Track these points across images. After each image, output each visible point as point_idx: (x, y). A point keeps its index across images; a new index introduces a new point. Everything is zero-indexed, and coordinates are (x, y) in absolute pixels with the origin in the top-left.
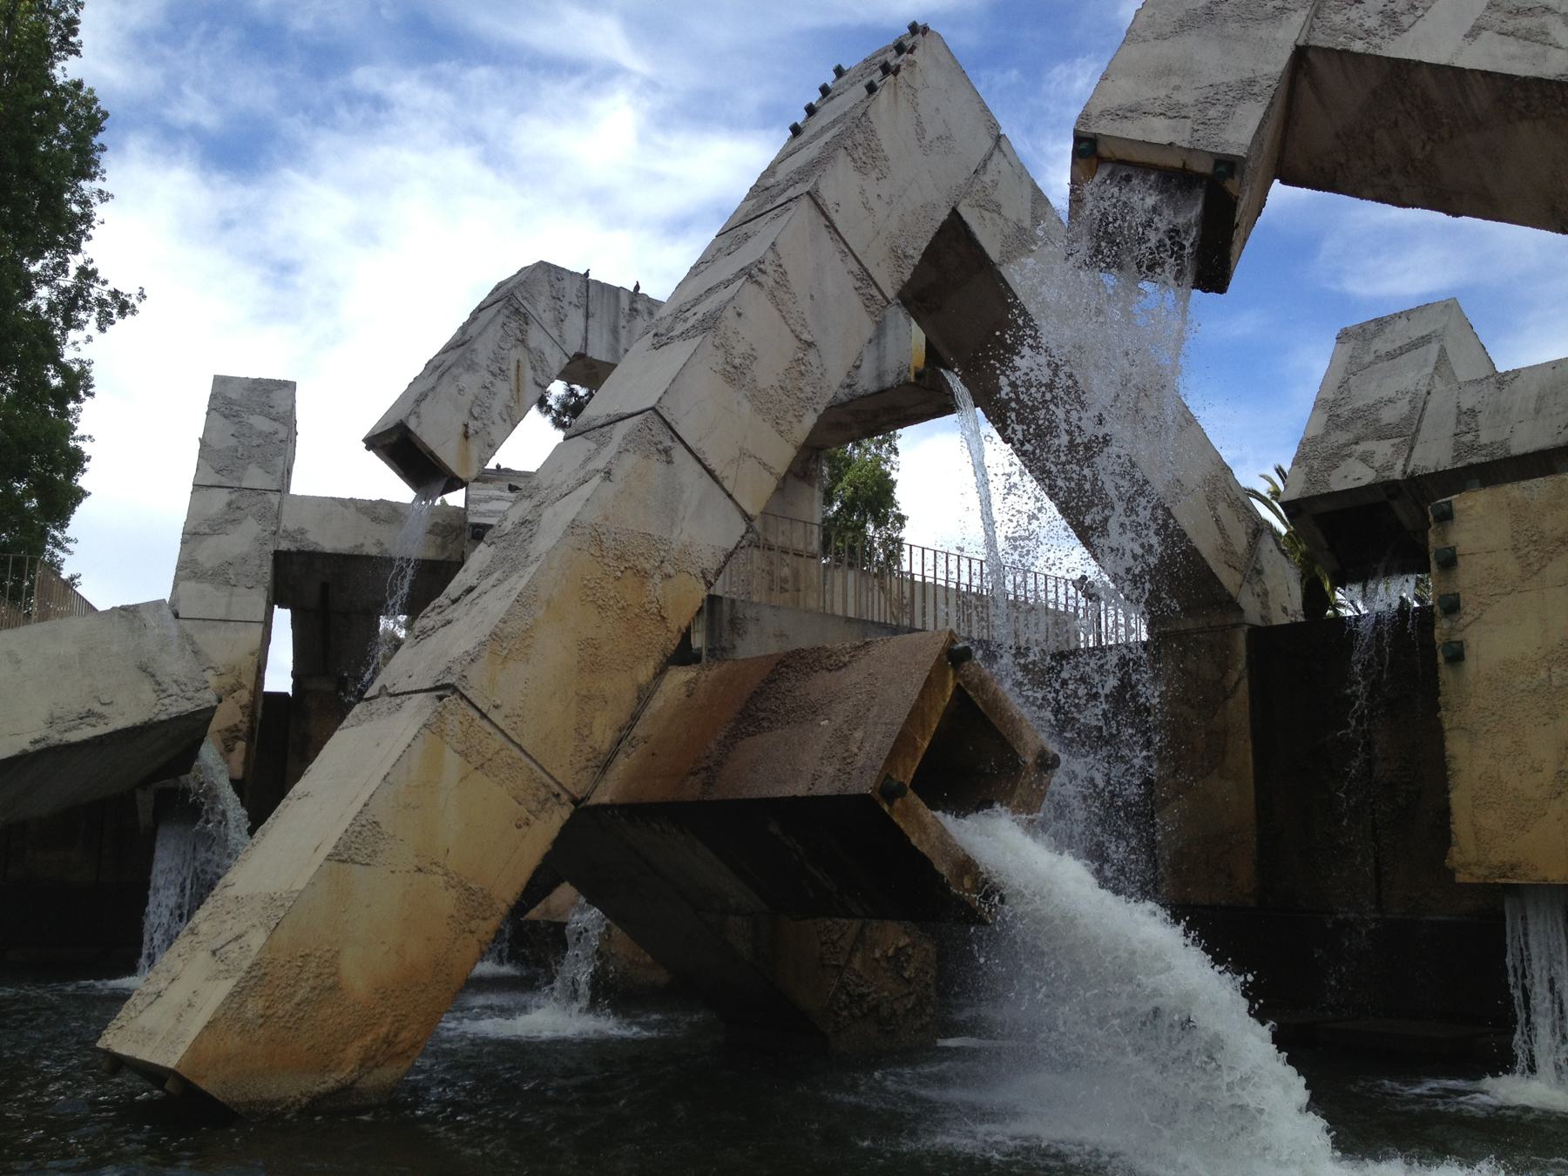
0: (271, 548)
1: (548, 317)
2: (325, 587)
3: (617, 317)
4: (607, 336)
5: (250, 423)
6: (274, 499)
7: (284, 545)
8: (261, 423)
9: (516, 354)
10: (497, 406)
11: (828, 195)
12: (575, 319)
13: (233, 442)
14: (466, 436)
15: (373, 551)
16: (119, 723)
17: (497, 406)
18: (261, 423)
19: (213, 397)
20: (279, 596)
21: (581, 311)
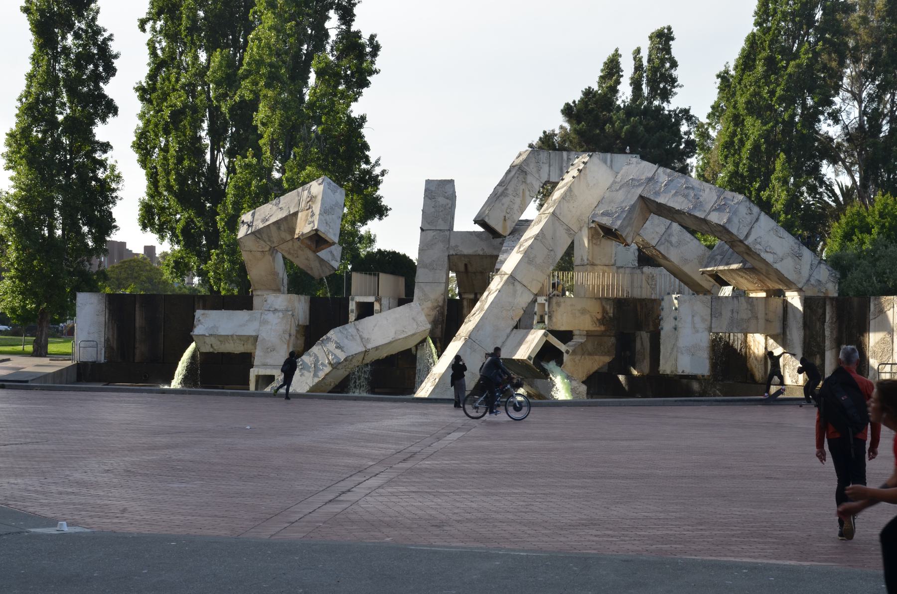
0: (447, 254)
1: (534, 170)
2: (466, 265)
3: (562, 163)
4: (558, 172)
5: (440, 196)
6: (447, 233)
7: (452, 252)
8: (441, 200)
9: (523, 187)
10: (516, 207)
11: (558, 212)
12: (545, 168)
13: (433, 210)
14: (505, 220)
15: (481, 253)
16: (410, 333)
17: (516, 207)
18: (441, 200)
19: (426, 190)
20: (451, 269)
21: (547, 165)
